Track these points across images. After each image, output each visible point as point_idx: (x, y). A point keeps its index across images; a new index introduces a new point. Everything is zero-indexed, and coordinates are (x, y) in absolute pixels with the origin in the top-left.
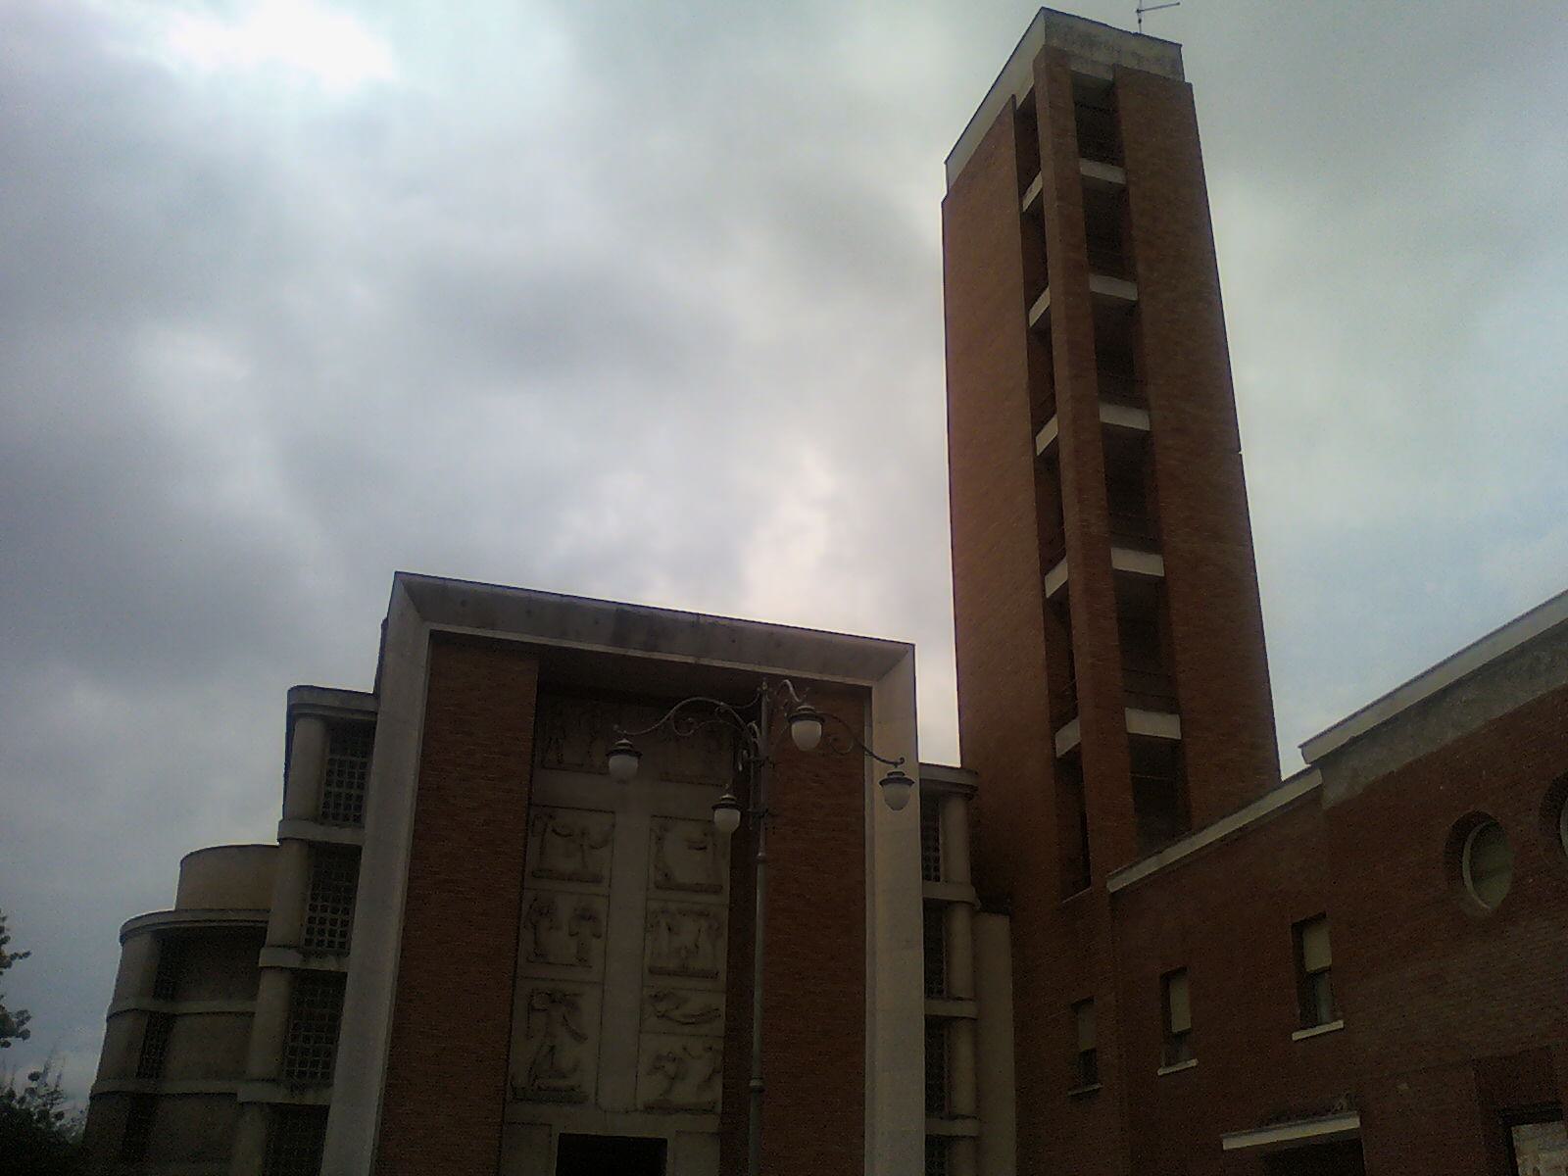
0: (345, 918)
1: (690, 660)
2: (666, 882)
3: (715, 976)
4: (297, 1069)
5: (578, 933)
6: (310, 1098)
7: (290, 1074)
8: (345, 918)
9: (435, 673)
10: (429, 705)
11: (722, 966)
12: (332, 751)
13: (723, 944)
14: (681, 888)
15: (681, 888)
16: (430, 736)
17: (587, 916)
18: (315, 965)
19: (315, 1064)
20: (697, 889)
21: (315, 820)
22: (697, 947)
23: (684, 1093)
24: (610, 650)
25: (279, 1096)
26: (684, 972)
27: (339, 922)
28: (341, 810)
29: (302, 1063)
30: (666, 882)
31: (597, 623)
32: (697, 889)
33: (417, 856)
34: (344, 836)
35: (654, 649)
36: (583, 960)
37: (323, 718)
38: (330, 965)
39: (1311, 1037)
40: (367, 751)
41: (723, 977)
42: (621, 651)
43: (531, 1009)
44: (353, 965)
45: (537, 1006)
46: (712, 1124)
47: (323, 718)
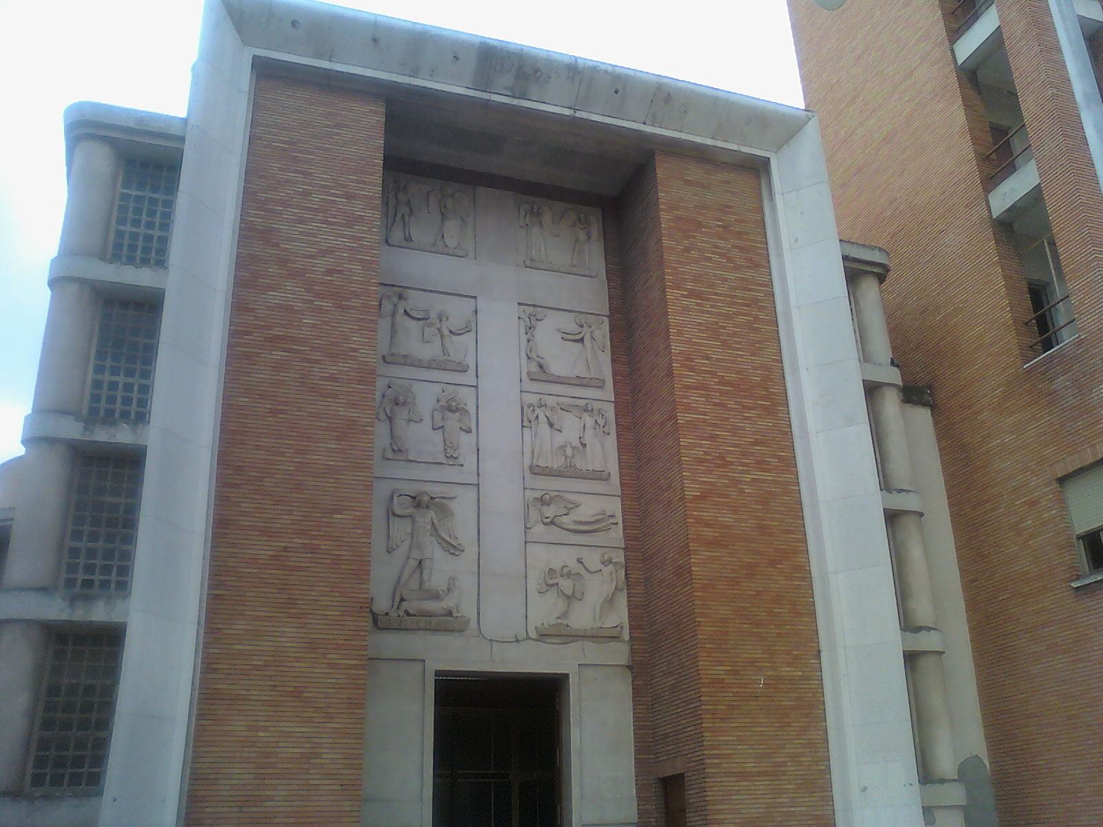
0: (143, 382)
1: (567, 112)
2: (541, 374)
3: (607, 478)
4: (80, 576)
5: (443, 426)
6: (99, 613)
7: (70, 583)
8: (143, 382)
9: (257, 106)
10: (252, 139)
11: (613, 467)
12: (126, 184)
13: (612, 442)
14: (559, 381)
15: (559, 381)
16: (253, 172)
17: (451, 407)
18: (102, 435)
19: (106, 570)
20: (580, 382)
21: (102, 258)
22: (584, 445)
23: (583, 617)
24: (471, 93)
25: (55, 610)
26: (569, 472)
27: (136, 388)
28: (118, 405)
29: (89, 568)
30: (541, 374)
31: (456, 58)
32: (580, 382)
33: (239, 307)
34: (140, 277)
35: (523, 97)
36: (452, 458)
37: (113, 143)
38: (123, 435)
39: (1095, 582)
40: (172, 186)
41: (615, 478)
42: (485, 96)
43: (391, 514)
44: (153, 438)
45: (558, 367)
46: (620, 653)
47: (113, 143)
